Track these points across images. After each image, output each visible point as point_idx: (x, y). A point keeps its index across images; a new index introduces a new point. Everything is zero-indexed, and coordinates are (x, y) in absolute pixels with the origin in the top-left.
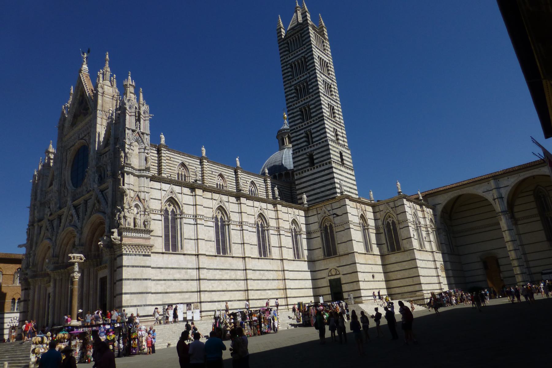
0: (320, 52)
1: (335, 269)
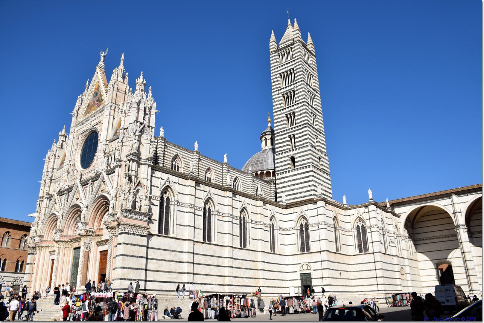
0: (307, 66)
1: (307, 265)
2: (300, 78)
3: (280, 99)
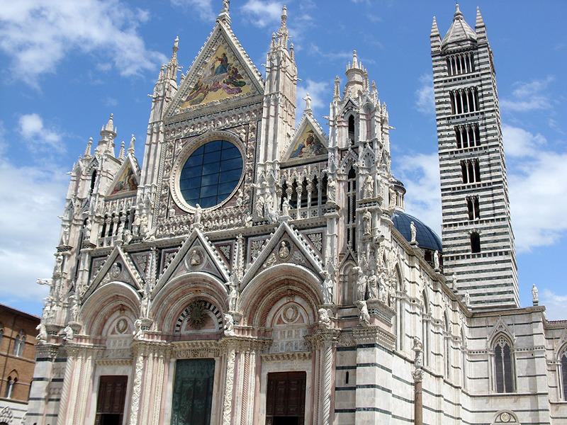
3: (451, 133)
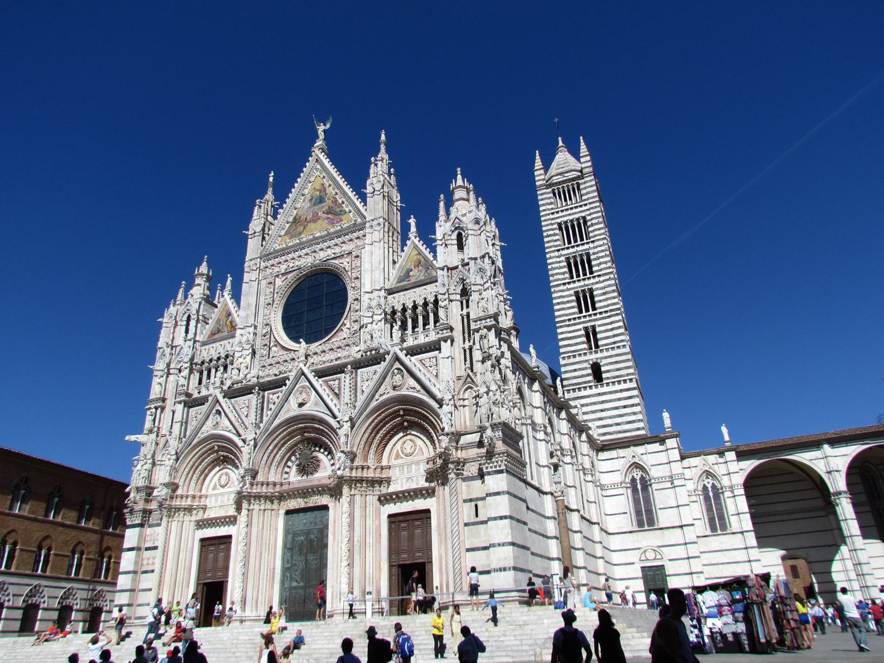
1: (654, 550)
2: (600, 235)
